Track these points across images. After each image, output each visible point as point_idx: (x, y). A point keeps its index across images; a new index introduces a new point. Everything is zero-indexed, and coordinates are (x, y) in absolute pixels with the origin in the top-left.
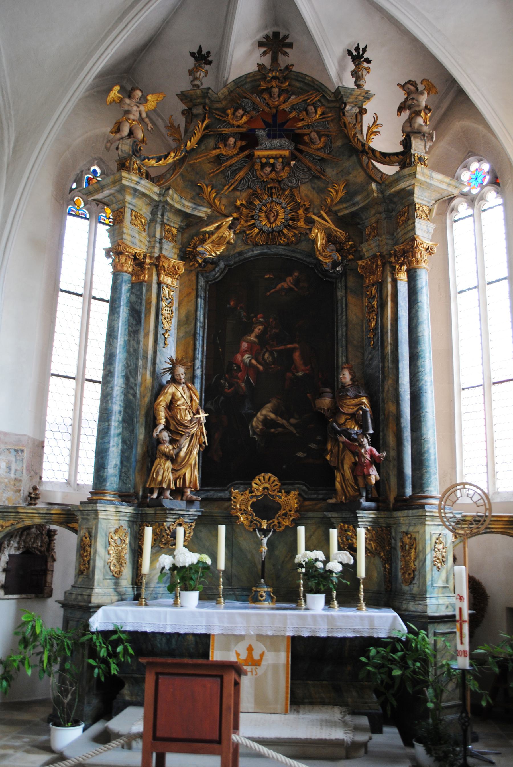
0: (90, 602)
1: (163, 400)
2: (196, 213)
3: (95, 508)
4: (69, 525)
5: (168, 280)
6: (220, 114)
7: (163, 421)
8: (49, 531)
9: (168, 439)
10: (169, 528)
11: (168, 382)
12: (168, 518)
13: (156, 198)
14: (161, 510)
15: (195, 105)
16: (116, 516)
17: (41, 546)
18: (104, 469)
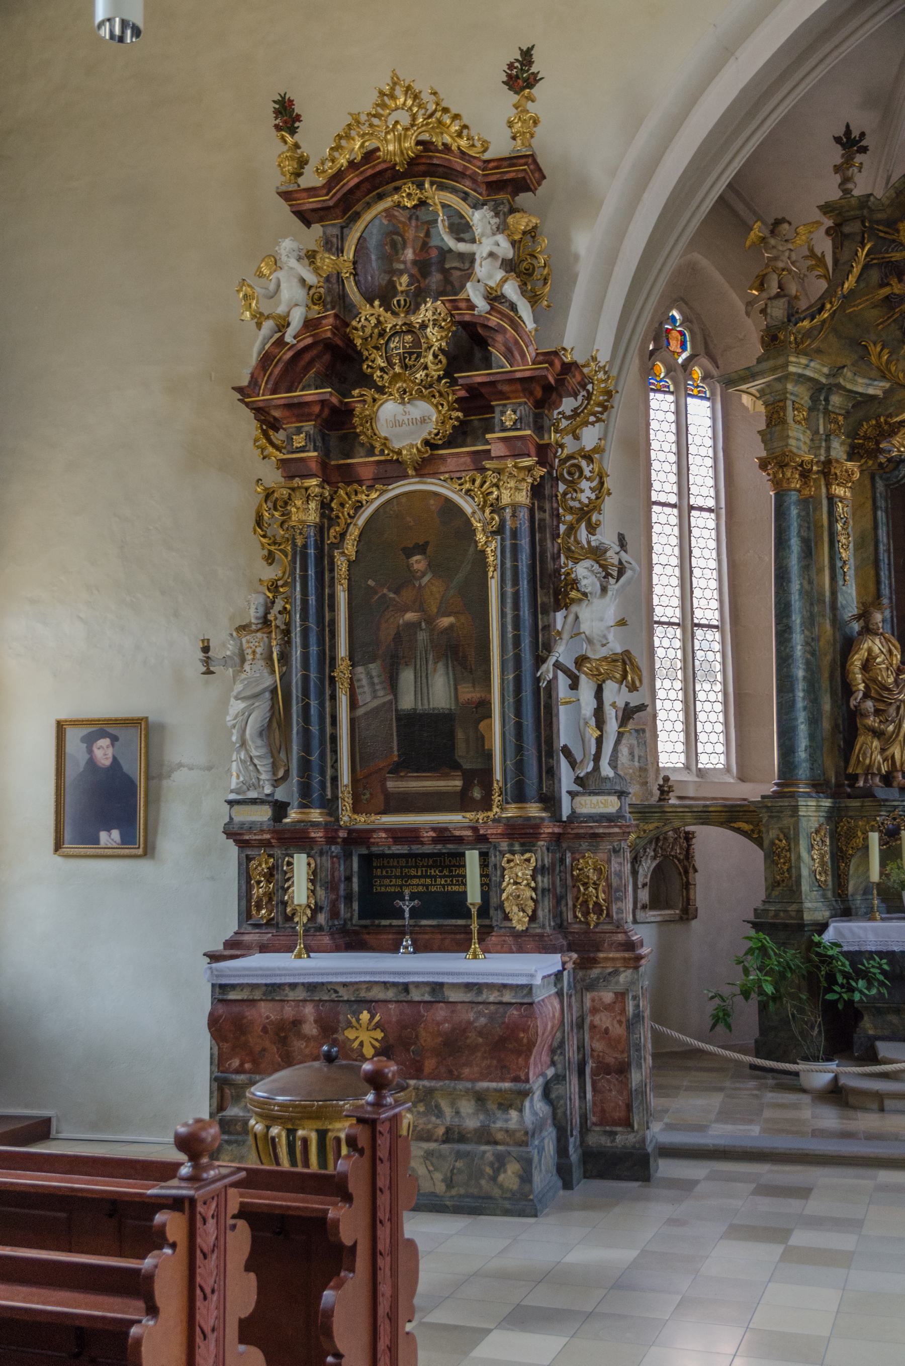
0: (802, 918)
1: (857, 660)
2: (871, 391)
3: (793, 804)
4: (732, 825)
5: (839, 491)
6: (886, 229)
7: (862, 687)
8: (687, 833)
9: (872, 710)
10: (883, 823)
11: (860, 633)
12: (881, 811)
13: (824, 380)
14: (872, 801)
15: (847, 220)
16: (816, 811)
17: (680, 853)
18: (794, 752)
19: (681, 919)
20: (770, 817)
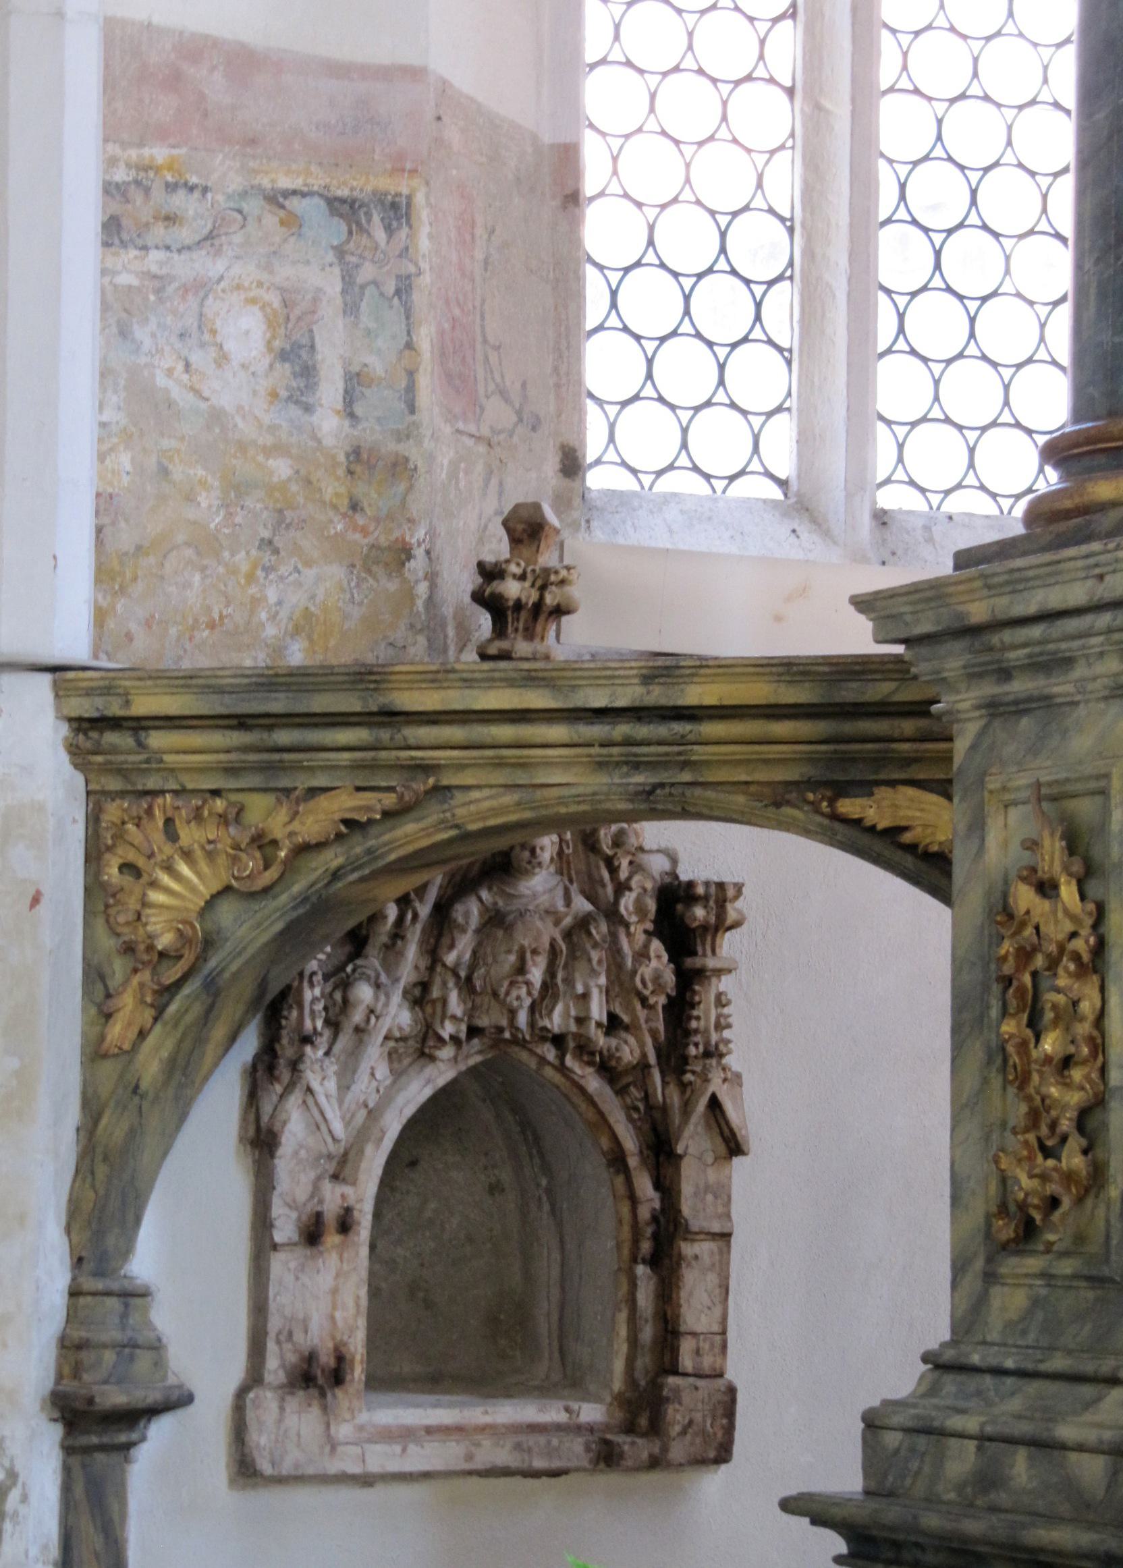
4: (849, 807)
8: (674, 898)
17: (613, 1024)
19: (607, 1456)
20: (994, 709)
